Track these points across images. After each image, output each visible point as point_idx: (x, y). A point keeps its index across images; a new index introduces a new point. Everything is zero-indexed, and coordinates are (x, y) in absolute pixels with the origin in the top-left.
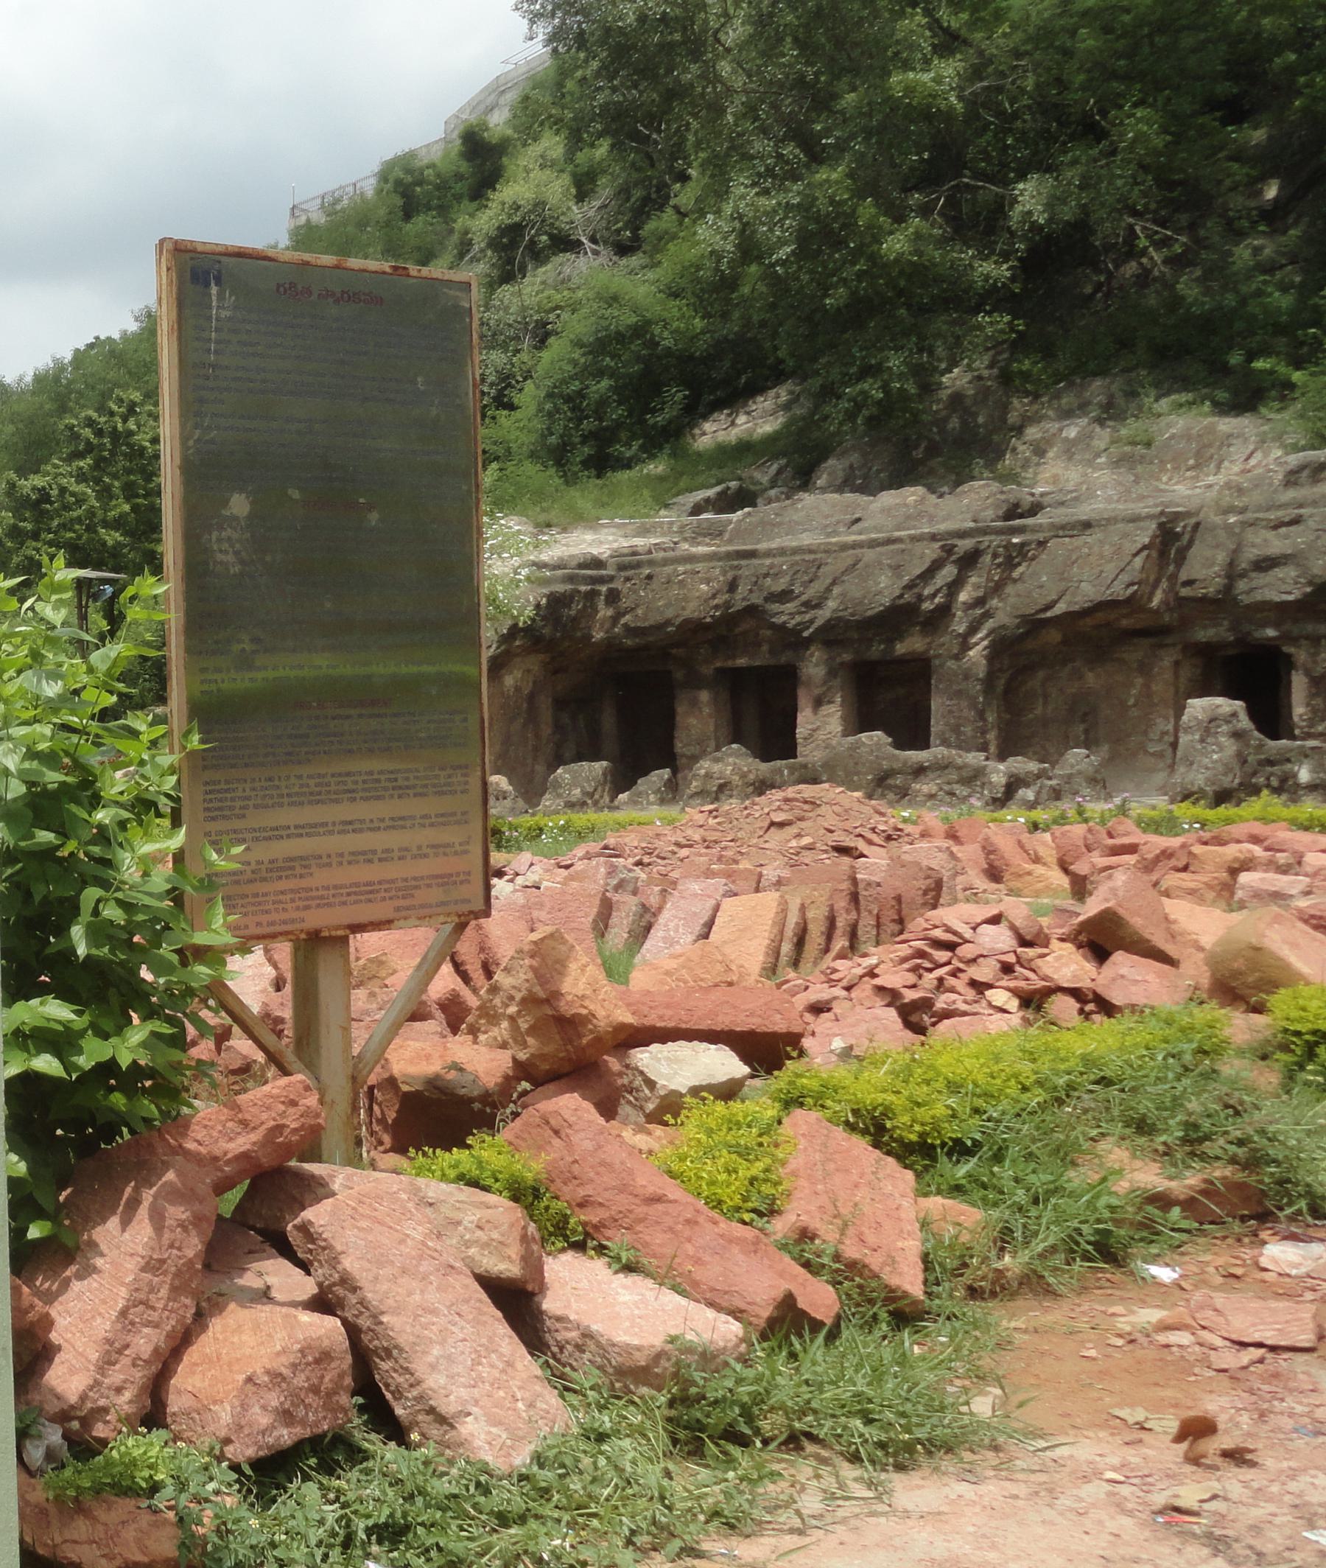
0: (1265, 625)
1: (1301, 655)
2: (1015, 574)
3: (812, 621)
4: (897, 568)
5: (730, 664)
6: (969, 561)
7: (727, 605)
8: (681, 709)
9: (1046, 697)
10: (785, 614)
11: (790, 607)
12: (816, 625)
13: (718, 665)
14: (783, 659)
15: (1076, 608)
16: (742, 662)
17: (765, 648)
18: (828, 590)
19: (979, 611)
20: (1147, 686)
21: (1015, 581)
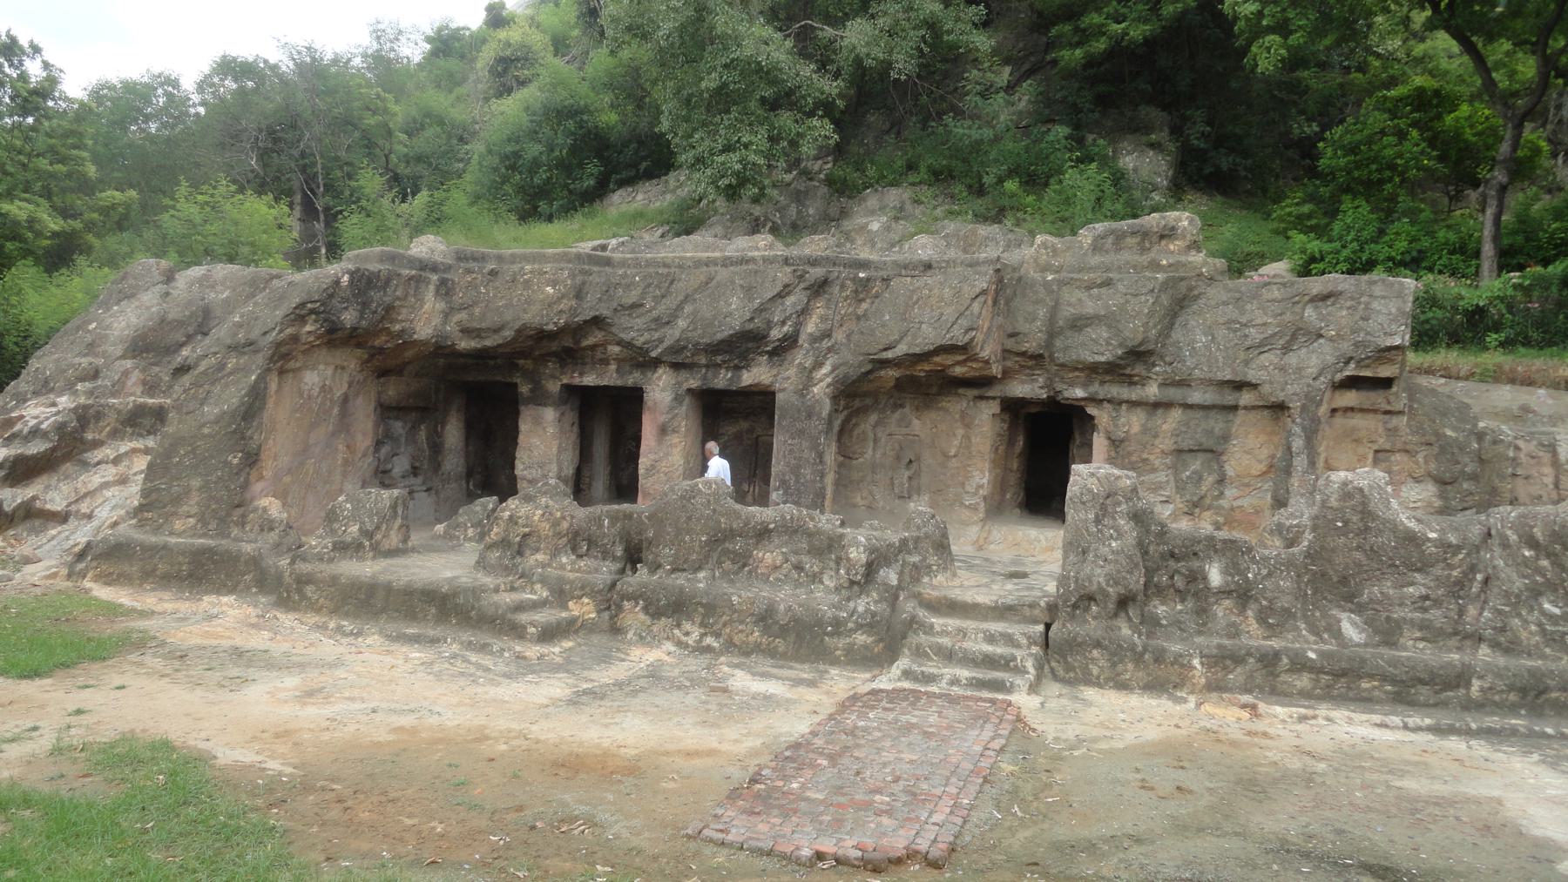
0: (1072, 385)
3: (661, 341)
4: (749, 290)
5: (577, 381)
6: (819, 288)
7: (574, 311)
8: (524, 427)
9: (876, 441)
10: (635, 330)
11: (639, 322)
12: (666, 344)
13: (565, 381)
14: (631, 380)
15: (917, 350)
16: (589, 380)
17: (613, 367)
18: (680, 307)
19: (826, 344)
20: (967, 437)
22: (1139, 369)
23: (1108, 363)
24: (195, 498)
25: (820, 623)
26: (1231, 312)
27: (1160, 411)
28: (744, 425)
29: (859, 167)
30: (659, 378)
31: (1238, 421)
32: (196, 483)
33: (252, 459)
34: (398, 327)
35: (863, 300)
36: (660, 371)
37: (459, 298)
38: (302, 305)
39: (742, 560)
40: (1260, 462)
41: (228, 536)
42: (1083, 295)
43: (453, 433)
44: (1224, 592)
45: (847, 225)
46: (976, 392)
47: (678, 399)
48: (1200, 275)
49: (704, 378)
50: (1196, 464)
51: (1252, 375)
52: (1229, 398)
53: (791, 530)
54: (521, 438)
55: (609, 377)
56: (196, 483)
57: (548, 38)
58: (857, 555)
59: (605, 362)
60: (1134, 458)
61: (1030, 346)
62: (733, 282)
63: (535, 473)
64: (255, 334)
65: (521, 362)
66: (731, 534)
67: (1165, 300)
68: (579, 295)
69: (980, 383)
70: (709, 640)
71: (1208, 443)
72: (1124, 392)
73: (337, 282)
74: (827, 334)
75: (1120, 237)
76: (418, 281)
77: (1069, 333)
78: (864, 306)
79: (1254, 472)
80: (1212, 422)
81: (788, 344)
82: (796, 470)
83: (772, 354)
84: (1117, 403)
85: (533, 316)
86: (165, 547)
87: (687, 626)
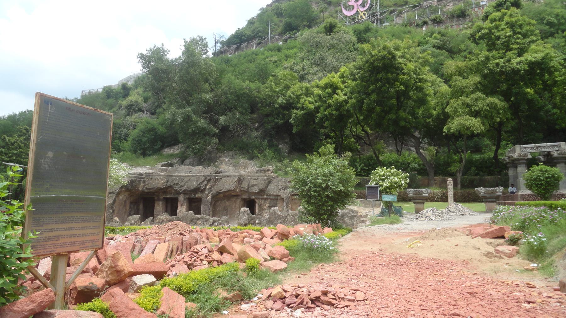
1: (257, 201)
4: (197, 181)
6: (209, 181)
8: (156, 205)
10: (177, 188)
11: (178, 186)
14: (176, 196)
16: (168, 196)
26: (277, 183)
28: (196, 204)
29: (224, 145)
33: (113, 211)
37: (146, 183)
43: (141, 207)
44: (258, 223)
45: (220, 159)
47: (184, 200)
51: (279, 194)
53: (202, 218)
55: (172, 196)
57: (142, 98)
58: (211, 221)
59: (171, 193)
61: (245, 189)
64: (114, 190)
67: (267, 181)
68: (167, 182)
69: (237, 196)
72: (260, 197)
74: (210, 188)
75: (261, 171)
76: (140, 181)
81: (204, 189)
85: (159, 186)
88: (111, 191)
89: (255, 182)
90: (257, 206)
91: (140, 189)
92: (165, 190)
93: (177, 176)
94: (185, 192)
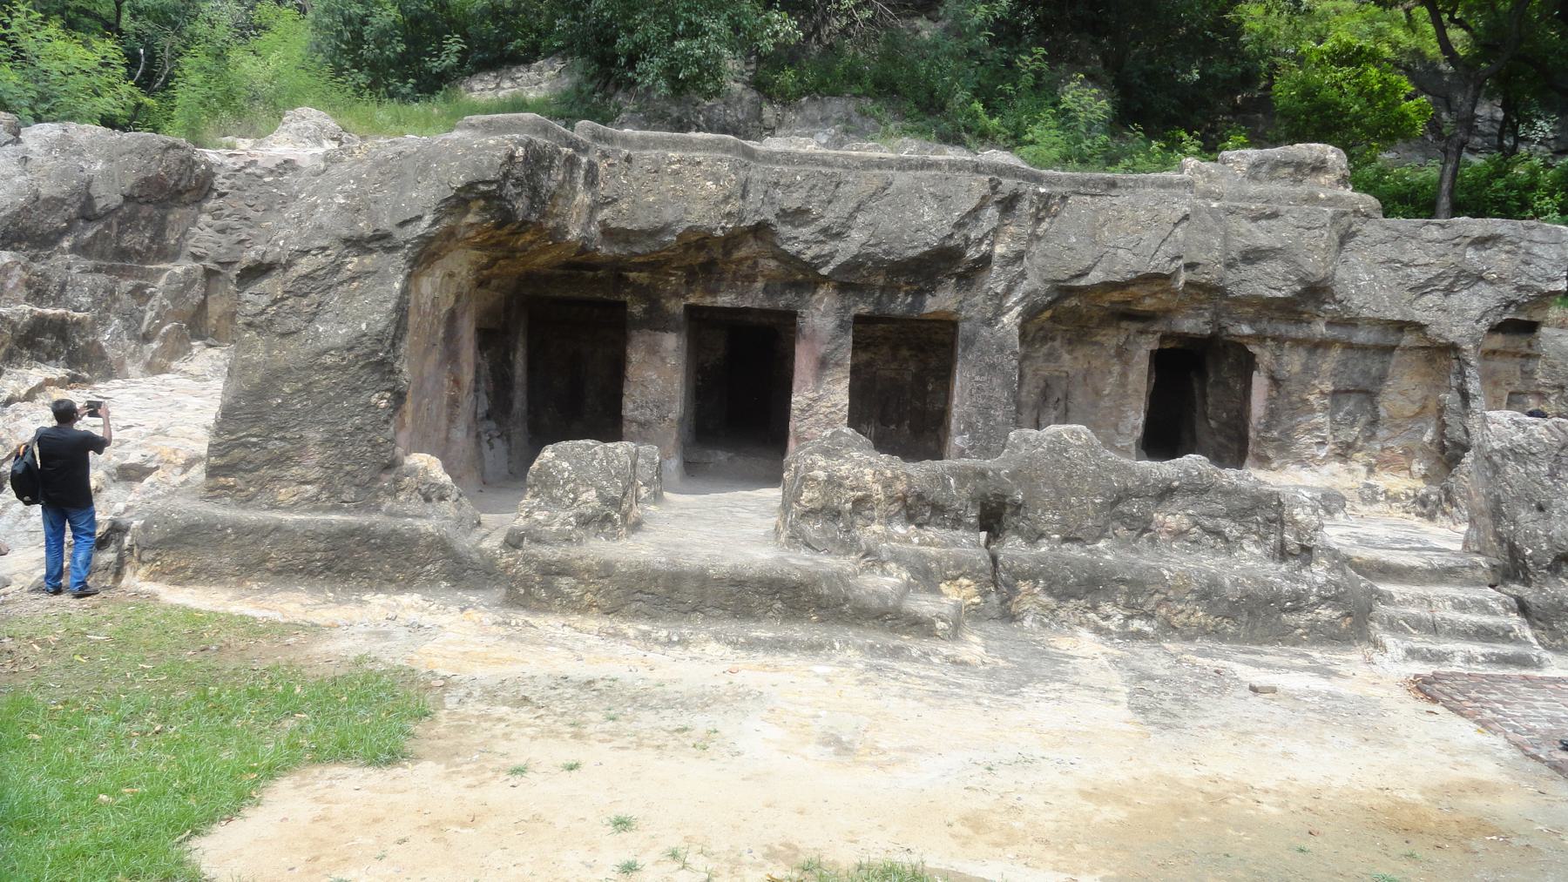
1: (1264, 355)
2: (1040, 231)
3: (832, 255)
4: (942, 199)
5: (708, 301)
8: (635, 356)
10: (799, 241)
11: (805, 232)
12: (840, 259)
13: (692, 301)
14: (781, 303)
15: (1117, 278)
16: (725, 300)
17: (759, 284)
18: (852, 216)
19: (1017, 269)
20: (1124, 375)
21: (1039, 238)
22: (1311, 307)
23: (1285, 299)
24: (314, 456)
25: (1276, 597)
26: (1390, 251)
27: (1320, 351)
30: (820, 301)
31: (1393, 362)
32: (314, 435)
34: (551, 224)
35: (1043, 219)
36: (821, 292)
37: (604, 190)
38: (471, 186)
39: (1143, 526)
40: (1413, 402)
41: (377, 509)
42: (1252, 226)
46: (1140, 326)
47: (842, 326)
48: (1356, 212)
49: (878, 302)
50: (1349, 406)
51: (1419, 316)
52: (1391, 339)
53: (1197, 489)
54: (631, 371)
55: (753, 298)
56: (314, 435)
59: (751, 278)
60: (1294, 399)
62: (919, 190)
63: (648, 414)
64: (386, 224)
65: (632, 275)
66: (1124, 495)
70: (1137, 624)
71: (1365, 383)
73: (511, 157)
77: (1241, 266)
78: (1044, 225)
79: (1407, 413)
80: (1368, 362)
82: (985, 412)
83: (960, 277)
84: (1279, 340)
86: (278, 528)
87: (1107, 608)
88: (364, 227)
89: (1261, 236)
90: (1259, 383)
91: (574, 233)
92: (705, 255)
93: (788, 158)
94: (849, 280)
